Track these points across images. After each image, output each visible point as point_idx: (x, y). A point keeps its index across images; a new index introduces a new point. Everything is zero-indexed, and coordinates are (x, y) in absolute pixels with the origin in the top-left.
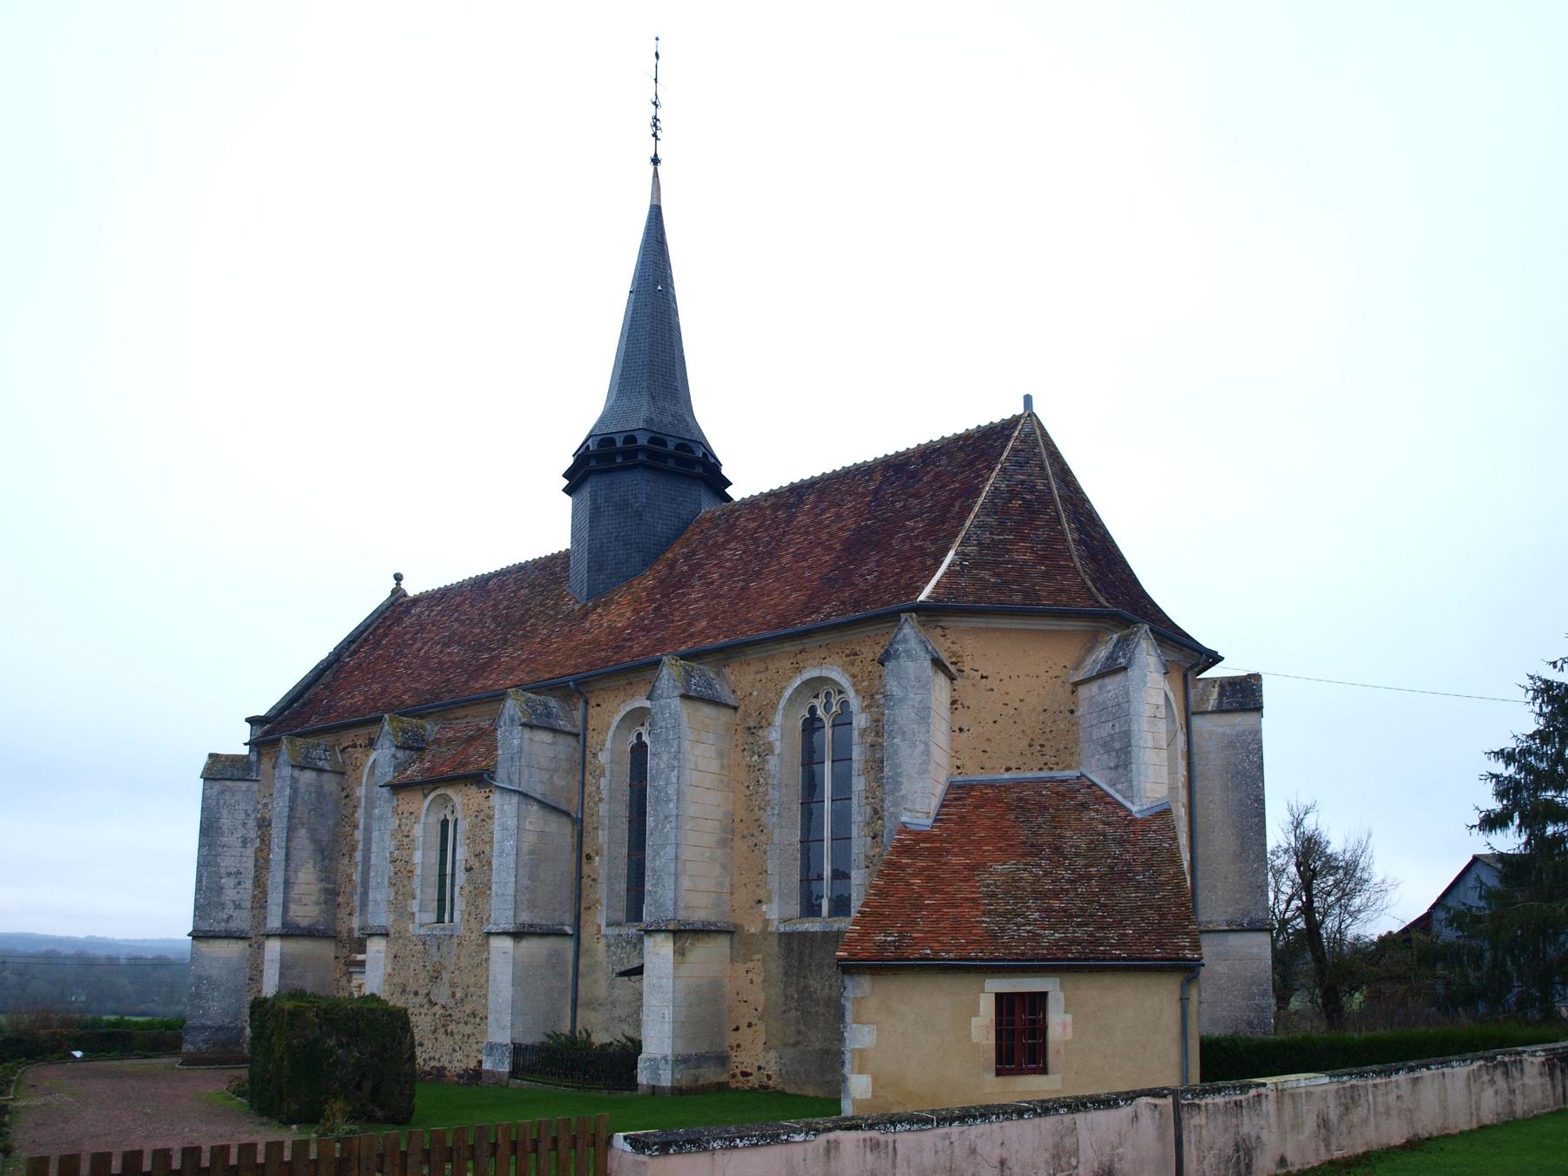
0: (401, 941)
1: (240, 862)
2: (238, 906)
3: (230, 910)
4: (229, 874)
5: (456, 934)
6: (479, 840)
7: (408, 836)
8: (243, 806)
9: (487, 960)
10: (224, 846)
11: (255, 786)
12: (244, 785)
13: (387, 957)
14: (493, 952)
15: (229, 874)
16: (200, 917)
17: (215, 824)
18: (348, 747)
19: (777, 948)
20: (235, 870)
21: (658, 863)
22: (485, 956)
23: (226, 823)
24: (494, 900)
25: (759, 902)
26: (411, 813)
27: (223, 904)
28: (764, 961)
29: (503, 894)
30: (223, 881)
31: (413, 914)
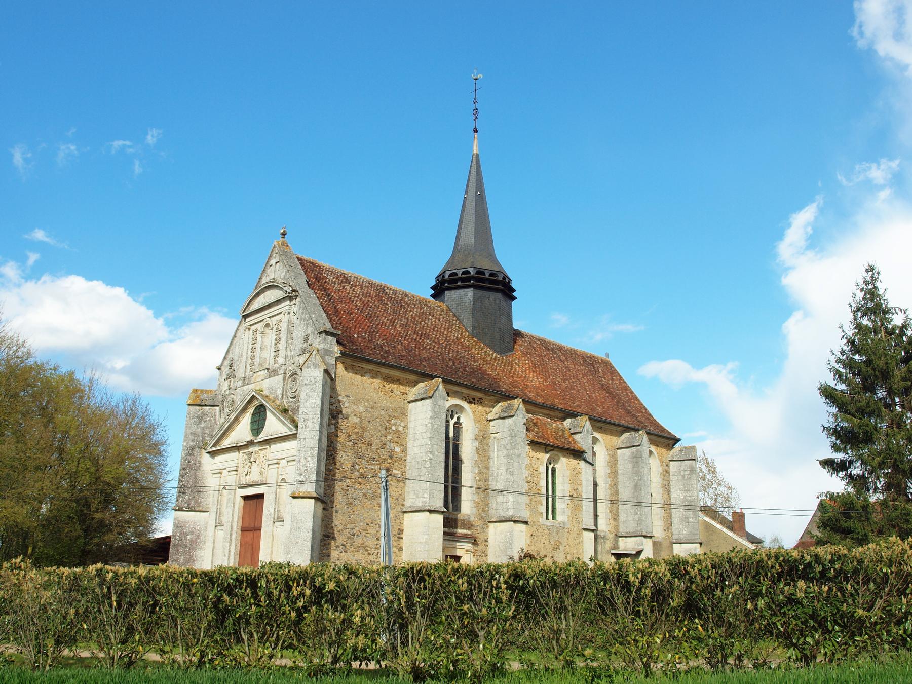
0: (535, 527)
5: (566, 527)
6: (575, 483)
7: (536, 471)
9: (582, 542)
14: (585, 538)
22: (581, 539)
24: (584, 513)
26: (538, 459)
29: (588, 511)
31: (542, 513)
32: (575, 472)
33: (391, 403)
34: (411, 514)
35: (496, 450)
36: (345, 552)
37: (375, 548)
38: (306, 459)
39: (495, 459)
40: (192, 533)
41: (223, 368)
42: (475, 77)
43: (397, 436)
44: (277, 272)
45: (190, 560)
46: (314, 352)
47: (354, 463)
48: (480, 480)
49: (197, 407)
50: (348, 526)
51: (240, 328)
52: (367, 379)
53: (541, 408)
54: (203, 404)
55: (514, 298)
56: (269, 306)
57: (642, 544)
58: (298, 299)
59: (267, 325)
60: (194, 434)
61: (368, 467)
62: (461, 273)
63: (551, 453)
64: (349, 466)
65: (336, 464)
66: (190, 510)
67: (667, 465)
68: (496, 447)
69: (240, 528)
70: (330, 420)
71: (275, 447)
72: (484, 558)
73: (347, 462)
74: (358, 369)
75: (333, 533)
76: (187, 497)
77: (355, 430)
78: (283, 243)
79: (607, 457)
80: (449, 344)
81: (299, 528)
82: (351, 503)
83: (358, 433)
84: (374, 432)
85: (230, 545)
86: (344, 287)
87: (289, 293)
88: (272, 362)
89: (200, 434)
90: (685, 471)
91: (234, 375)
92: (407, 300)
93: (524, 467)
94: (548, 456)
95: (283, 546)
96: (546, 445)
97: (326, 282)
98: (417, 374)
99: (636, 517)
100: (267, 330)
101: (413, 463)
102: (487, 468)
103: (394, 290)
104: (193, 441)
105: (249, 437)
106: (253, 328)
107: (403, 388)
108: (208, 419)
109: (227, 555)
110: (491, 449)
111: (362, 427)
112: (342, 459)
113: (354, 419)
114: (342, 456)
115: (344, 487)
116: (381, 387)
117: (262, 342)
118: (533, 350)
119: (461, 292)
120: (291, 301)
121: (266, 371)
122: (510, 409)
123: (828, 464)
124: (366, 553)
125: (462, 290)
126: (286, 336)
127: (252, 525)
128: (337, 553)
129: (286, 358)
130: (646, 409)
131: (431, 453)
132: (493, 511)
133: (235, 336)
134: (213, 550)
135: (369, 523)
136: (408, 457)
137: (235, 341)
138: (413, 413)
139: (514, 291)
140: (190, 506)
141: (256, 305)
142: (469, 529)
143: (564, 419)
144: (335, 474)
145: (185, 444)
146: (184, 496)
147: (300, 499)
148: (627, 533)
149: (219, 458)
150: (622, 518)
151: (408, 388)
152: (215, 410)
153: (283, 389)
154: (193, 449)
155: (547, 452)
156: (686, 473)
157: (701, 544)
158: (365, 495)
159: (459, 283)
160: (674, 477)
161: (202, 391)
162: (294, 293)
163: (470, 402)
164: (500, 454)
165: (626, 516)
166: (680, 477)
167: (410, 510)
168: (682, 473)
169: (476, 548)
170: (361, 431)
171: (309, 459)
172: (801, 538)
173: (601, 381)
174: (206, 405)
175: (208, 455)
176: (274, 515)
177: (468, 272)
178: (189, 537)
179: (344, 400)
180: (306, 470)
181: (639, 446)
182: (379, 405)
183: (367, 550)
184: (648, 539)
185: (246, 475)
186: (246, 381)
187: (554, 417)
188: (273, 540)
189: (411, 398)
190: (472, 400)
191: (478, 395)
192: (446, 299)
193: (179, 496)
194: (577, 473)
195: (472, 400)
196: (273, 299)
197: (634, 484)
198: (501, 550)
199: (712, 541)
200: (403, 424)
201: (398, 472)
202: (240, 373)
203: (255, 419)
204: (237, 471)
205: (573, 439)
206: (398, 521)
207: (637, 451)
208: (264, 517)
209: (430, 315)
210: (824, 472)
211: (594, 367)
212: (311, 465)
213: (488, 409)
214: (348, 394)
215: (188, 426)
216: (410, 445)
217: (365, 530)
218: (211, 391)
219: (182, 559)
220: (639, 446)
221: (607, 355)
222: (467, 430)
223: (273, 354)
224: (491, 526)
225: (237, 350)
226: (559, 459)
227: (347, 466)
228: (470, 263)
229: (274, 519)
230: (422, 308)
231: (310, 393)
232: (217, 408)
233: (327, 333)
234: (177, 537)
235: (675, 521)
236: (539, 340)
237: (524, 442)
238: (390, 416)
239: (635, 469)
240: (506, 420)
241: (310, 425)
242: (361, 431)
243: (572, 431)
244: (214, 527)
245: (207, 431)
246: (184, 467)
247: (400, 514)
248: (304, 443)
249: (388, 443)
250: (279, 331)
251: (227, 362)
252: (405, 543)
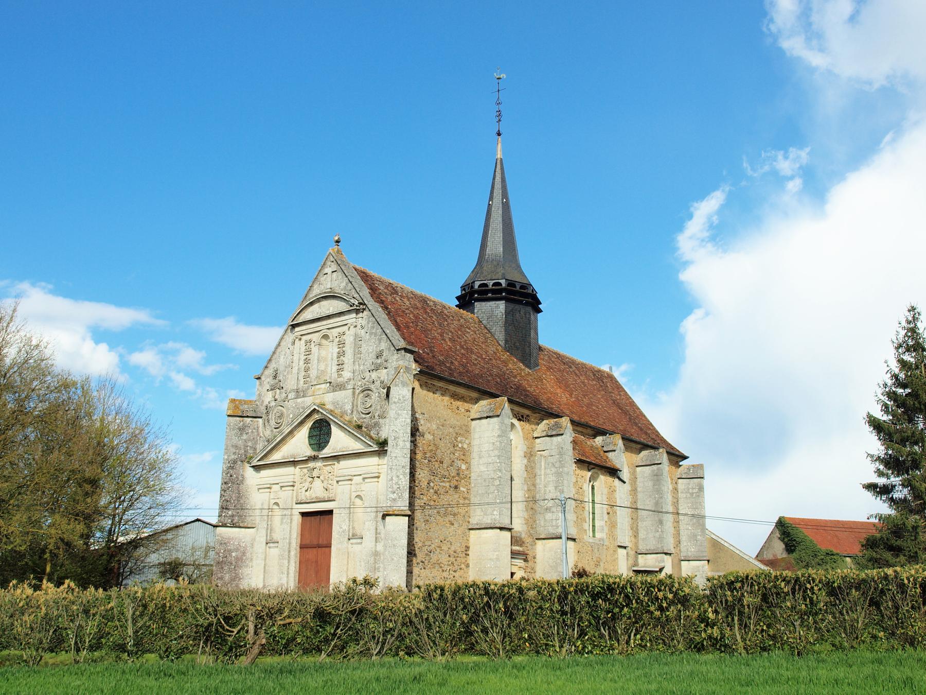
9: (617, 558)
13: (574, 552)
14: (619, 554)
24: (618, 530)
26: (582, 477)
31: (586, 530)
32: (611, 490)
34: (478, 531)
35: (543, 467)
36: (424, 568)
37: (448, 565)
38: (398, 477)
39: (543, 477)
40: (237, 550)
41: (263, 378)
42: (497, 77)
43: (462, 453)
44: (332, 281)
45: (236, 578)
46: (402, 371)
47: (429, 481)
48: (528, 498)
49: (238, 418)
50: (426, 543)
51: (285, 337)
52: (437, 396)
53: (577, 426)
54: (245, 415)
55: (539, 311)
56: (328, 317)
57: (663, 561)
58: (365, 313)
59: (326, 337)
60: (236, 447)
61: (441, 484)
62: (491, 284)
63: (592, 471)
64: (426, 484)
65: (415, 482)
66: (234, 526)
67: (676, 483)
68: (543, 464)
69: (299, 545)
71: (344, 463)
72: (533, 574)
73: (424, 480)
74: (430, 386)
75: (414, 550)
76: (230, 513)
77: (430, 448)
78: (338, 251)
79: (629, 474)
80: (490, 359)
81: (394, 545)
82: (428, 521)
85: (289, 562)
86: (395, 298)
87: (357, 306)
88: (335, 375)
89: (242, 447)
90: (693, 489)
91: (280, 386)
92: (446, 312)
93: (572, 485)
94: (590, 473)
95: (363, 563)
96: (590, 463)
97: (380, 293)
98: (479, 391)
99: (657, 535)
100: (324, 342)
101: (479, 481)
102: (534, 485)
103: (433, 302)
104: (234, 453)
105: (309, 452)
106: (304, 338)
107: (467, 406)
108: (250, 431)
109: (286, 573)
110: (538, 466)
111: (435, 445)
112: (420, 476)
113: (428, 437)
114: (420, 474)
115: (422, 504)
116: (450, 404)
117: (319, 354)
118: (553, 365)
119: (492, 304)
120: (357, 314)
121: (328, 384)
122: (558, 427)
123: (871, 487)
124: (441, 570)
125: (494, 302)
126: (352, 350)
127: (315, 542)
128: (418, 569)
129: (354, 373)
130: (653, 426)
131: (500, 471)
132: (541, 528)
133: (279, 345)
134: (265, 567)
135: (443, 540)
136: (472, 474)
137: (278, 350)
138: (478, 430)
139: (540, 303)
140: (234, 522)
141: (308, 315)
142: (521, 546)
143: (595, 436)
144: (415, 491)
145: (226, 457)
146: (227, 511)
147: (394, 517)
148: (647, 550)
149: (265, 473)
150: (642, 535)
151: (471, 406)
152: (258, 421)
153: (353, 404)
154: (235, 462)
155: (589, 470)
156: (694, 491)
157: (708, 561)
158: (438, 512)
159: (490, 295)
160: (682, 495)
161: (240, 401)
162: (361, 306)
163: (519, 420)
164: (548, 471)
165: (645, 533)
166: (689, 495)
167: (478, 527)
168: (691, 491)
169: (527, 565)
170: (434, 449)
171: (401, 477)
172: (757, 556)
173: (612, 396)
174: (248, 417)
175: (252, 469)
176: (349, 531)
177: (500, 284)
178: (234, 554)
179: (420, 417)
180: (399, 488)
181: (660, 464)
182: (448, 422)
183: (441, 567)
184: (668, 556)
185: (306, 491)
186: (299, 393)
187: (586, 435)
188: (348, 557)
189: (474, 415)
190: (521, 418)
191: (526, 412)
192: (476, 311)
193: (222, 512)
194: (612, 491)
195: (521, 418)
196: (331, 311)
197: (654, 501)
198: (551, 567)
199: (720, 558)
200: (467, 442)
201: (464, 490)
202: (290, 383)
203: (315, 433)
204: (293, 486)
205: (607, 457)
206: (465, 538)
207: (658, 469)
208: (333, 533)
209: (467, 327)
210: (869, 495)
211: (603, 382)
212: (403, 483)
213: (533, 426)
214: (423, 412)
215: (228, 438)
216: (474, 462)
217: (440, 547)
218: (250, 401)
219: (227, 577)
220: (660, 464)
221: (611, 368)
222: (517, 447)
223: (335, 368)
224: (539, 543)
225: (282, 360)
226: (598, 476)
227: (424, 484)
228: (500, 274)
229: (349, 536)
230: (459, 320)
231: (399, 412)
232: (260, 420)
233: (407, 350)
234: (221, 555)
235: (684, 538)
236: (555, 353)
237: (571, 460)
238: (457, 434)
239: (656, 487)
240: (554, 439)
241: (401, 443)
243: (605, 449)
244: (265, 544)
245: (250, 444)
246: (226, 481)
247: (467, 531)
248: (396, 461)
249: (456, 460)
250: (341, 344)
251: (269, 372)
252: (472, 559)
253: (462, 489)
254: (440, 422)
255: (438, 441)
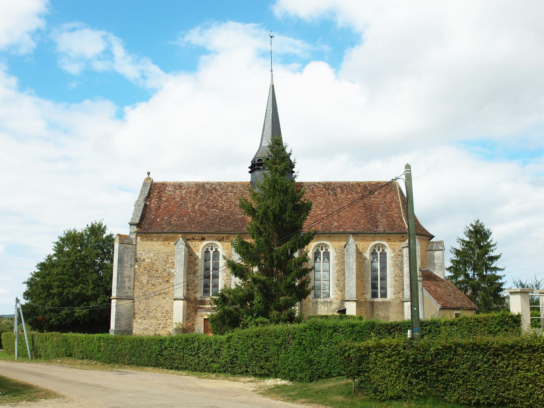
1: (130, 273)
2: (129, 288)
3: (127, 290)
4: (127, 277)
8: (130, 253)
10: (125, 267)
11: (134, 246)
12: (131, 246)
15: (127, 277)
16: (118, 292)
17: (122, 259)
18: (191, 239)
19: (369, 305)
20: (128, 276)
21: (350, 284)
23: (126, 259)
25: (364, 294)
27: (125, 287)
28: (365, 308)
30: (125, 279)
33: (169, 249)
36: (145, 320)
48: (227, 280)
70: (135, 263)
79: (335, 254)
83: (150, 266)
84: (159, 265)
111: (152, 263)
113: (147, 260)
124: (156, 320)
163: (220, 240)
183: (157, 318)
195: (221, 239)
238: (168, 256)
242: (152, 265)
253: (171, 281)
254: (156, 252)
255: (154, 262)
